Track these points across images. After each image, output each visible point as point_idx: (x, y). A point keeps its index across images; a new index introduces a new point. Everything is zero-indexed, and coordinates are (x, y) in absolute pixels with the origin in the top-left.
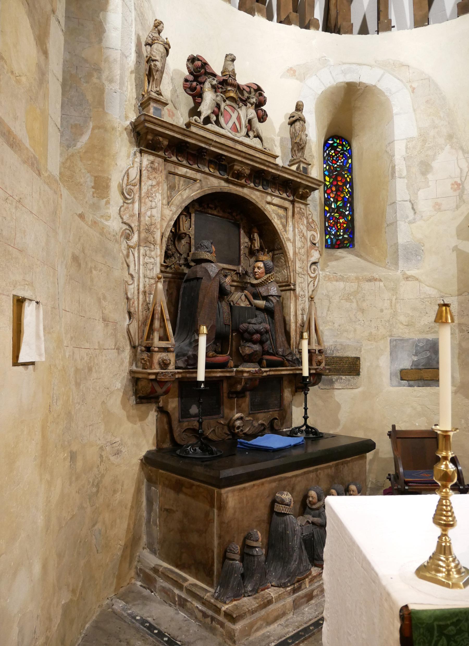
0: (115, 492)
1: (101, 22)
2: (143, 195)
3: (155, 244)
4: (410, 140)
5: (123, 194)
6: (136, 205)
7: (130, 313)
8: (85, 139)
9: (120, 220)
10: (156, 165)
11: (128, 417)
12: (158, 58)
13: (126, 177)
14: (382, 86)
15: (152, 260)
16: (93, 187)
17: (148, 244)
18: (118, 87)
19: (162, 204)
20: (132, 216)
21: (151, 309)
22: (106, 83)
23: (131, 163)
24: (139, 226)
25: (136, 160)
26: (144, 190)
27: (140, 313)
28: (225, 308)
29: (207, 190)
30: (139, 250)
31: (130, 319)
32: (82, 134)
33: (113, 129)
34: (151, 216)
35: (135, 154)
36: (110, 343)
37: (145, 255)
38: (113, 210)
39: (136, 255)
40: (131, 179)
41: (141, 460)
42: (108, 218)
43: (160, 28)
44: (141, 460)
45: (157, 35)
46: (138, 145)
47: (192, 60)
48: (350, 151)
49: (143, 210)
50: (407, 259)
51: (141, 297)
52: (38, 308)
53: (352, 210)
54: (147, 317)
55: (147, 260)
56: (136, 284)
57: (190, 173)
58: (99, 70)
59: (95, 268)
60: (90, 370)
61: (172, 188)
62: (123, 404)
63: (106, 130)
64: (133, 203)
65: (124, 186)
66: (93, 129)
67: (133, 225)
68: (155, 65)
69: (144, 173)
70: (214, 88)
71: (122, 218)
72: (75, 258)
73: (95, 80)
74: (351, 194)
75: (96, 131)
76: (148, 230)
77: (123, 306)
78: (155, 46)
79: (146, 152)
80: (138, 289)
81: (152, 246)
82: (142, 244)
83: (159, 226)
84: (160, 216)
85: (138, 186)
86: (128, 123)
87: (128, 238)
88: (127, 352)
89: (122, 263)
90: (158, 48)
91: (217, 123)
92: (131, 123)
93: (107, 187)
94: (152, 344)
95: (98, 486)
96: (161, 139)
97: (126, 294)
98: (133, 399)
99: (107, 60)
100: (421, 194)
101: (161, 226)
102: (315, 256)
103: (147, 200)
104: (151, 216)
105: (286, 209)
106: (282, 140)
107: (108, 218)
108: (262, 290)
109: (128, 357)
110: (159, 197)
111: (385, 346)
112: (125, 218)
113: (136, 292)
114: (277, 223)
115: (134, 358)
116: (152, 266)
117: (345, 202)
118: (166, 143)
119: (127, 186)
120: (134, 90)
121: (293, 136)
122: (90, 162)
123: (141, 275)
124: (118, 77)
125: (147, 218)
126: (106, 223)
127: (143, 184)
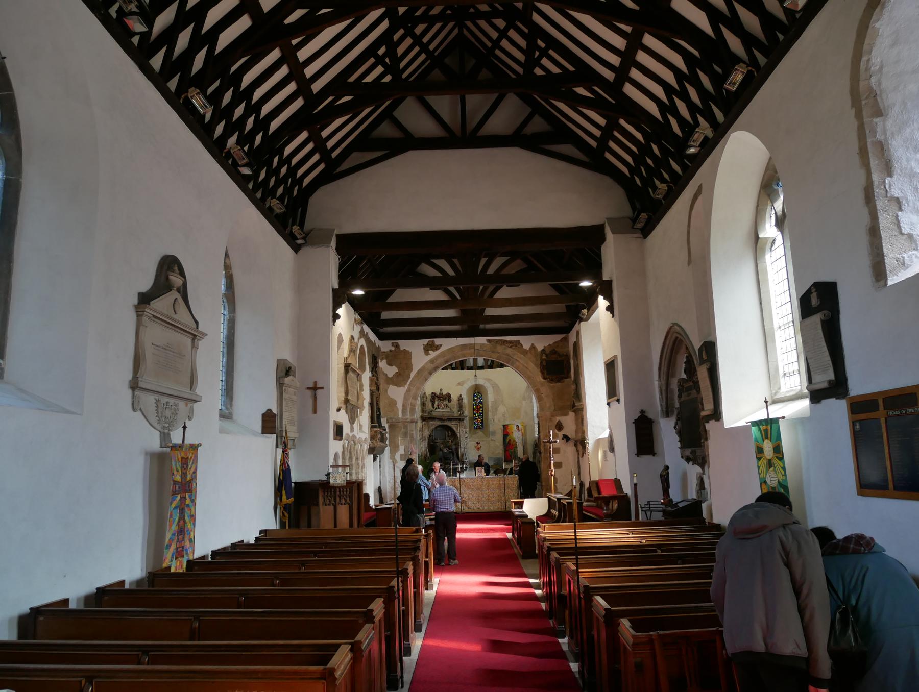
14: (485, 385)
46: (422, 419)
47: (433, 393)
48: (482, 397)
50: (492, 435)
53: (482, 416)
61: (429, 427)
74: (482, 411)
76: (424, 437)
91: (439, 408)
100: (495, 417)
102: (466, 435)
105: (457, 425)
106: (457, 404)
108: (451, 447)
114: (455, 429)
117: (480, 414)
121: (459, 404)
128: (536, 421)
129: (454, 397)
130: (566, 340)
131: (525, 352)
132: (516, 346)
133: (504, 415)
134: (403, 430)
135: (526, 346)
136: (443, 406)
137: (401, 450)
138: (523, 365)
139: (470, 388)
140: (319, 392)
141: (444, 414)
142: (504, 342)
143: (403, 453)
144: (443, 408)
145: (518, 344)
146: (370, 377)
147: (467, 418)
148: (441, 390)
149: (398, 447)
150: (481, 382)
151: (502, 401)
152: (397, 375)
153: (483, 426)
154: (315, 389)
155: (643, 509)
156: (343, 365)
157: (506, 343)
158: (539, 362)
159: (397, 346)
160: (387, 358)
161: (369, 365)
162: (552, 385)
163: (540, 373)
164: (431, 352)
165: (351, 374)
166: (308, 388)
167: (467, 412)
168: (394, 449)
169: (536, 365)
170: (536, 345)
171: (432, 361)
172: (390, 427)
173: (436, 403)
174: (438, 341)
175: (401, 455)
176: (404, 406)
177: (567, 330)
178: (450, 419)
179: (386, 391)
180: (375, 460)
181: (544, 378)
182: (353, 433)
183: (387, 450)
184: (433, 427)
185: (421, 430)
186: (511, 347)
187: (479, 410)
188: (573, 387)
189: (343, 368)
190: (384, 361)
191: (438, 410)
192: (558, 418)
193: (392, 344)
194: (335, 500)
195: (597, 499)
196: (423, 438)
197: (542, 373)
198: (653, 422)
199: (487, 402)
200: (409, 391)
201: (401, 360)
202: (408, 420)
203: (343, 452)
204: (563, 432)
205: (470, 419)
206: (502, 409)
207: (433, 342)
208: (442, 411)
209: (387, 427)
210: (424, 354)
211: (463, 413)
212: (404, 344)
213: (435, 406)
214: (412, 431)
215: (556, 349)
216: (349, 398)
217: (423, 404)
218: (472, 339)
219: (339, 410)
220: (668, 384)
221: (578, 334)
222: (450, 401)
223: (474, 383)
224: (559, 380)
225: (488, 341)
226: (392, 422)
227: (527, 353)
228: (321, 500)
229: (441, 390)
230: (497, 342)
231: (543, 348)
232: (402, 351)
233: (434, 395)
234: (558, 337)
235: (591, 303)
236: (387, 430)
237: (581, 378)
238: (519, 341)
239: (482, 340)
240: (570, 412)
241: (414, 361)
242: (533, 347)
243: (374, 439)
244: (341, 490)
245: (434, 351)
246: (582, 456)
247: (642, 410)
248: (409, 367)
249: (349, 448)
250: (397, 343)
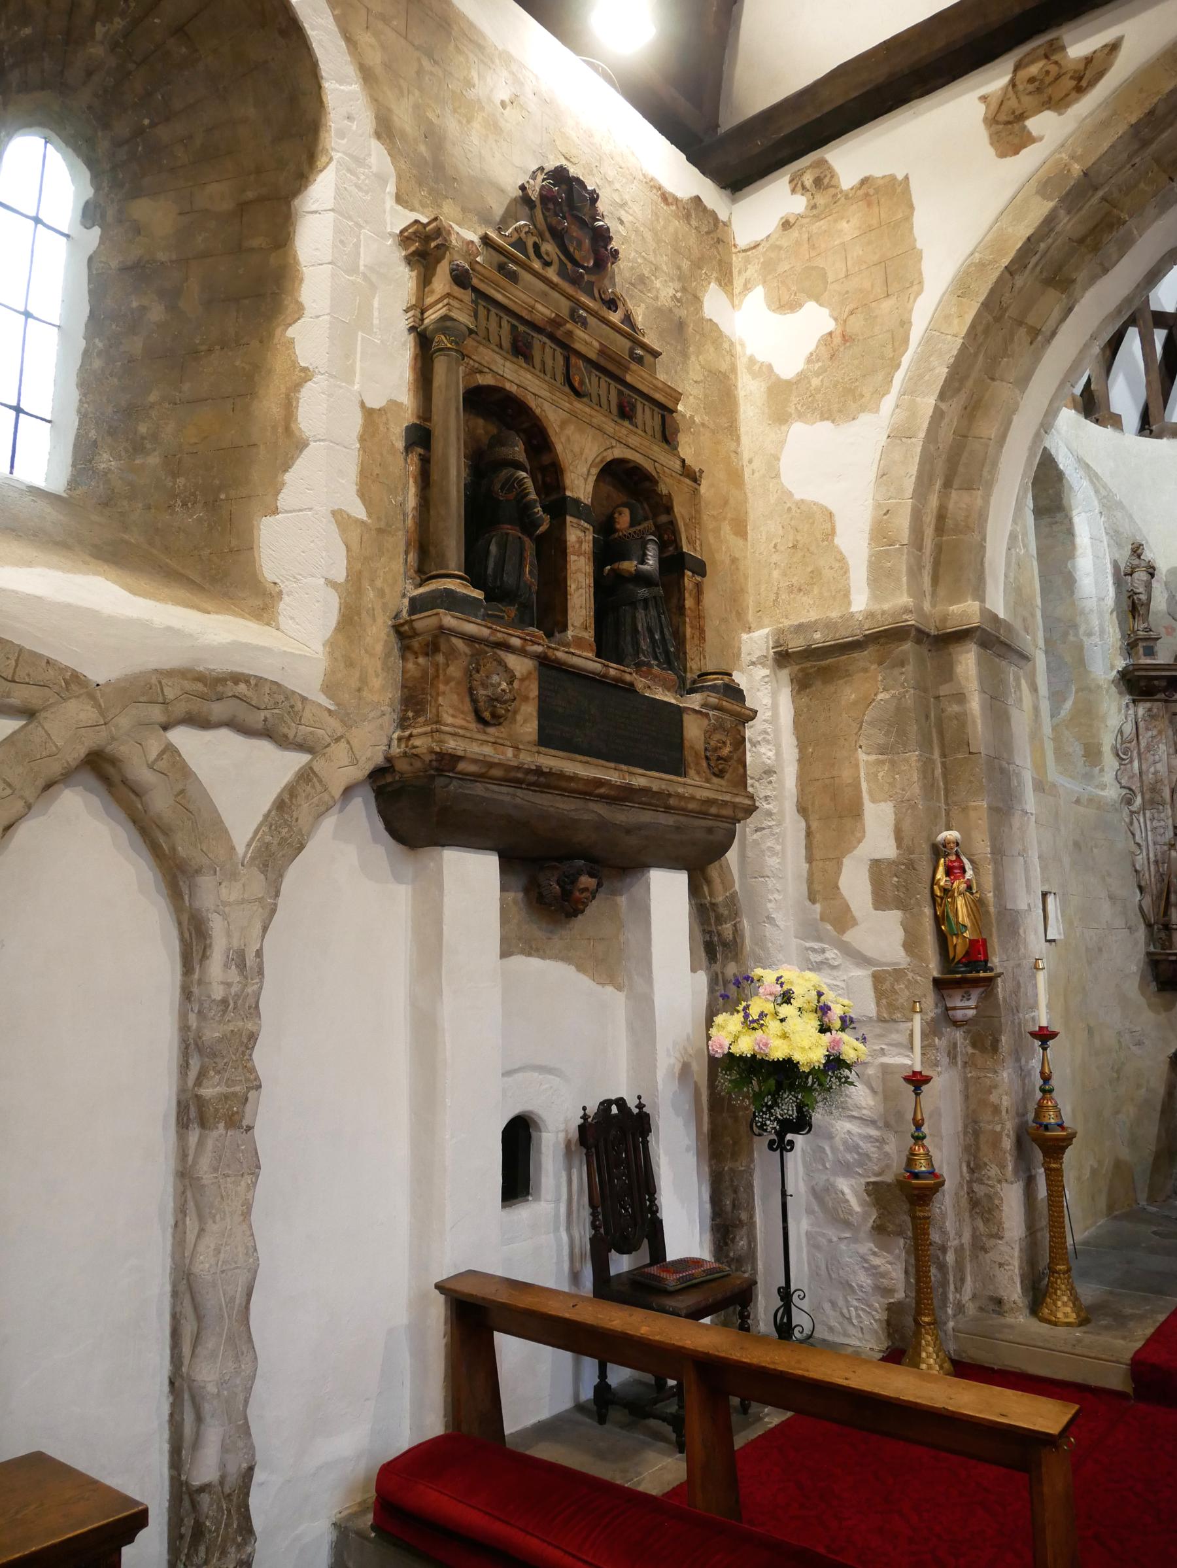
0: (1139, 1086)
1: (1070, 572)
2: (1142, 750)
3: (1163, 804)
5: (1118, 755)
6: (1136, 764)
7: (1141, 888)
8: (1068, 704)
9: (1118, 786)
10: (1155, 710)
11: (1149, 1005)
12: (1141, 590)
13: (1119, 736)
15: (1162, 823)
16: (1084, 756)
17: (1156, 806)
18: (1098, 640)
19: (1168, 755)
20: (1131, 777)
21: (1166, 881)
22: (1085, 639)
23: (1123, 717)
24: (1142, 786)
25: (1130, 712)
26: (1143, 744)
27: (1154, 887)
30: (1144, 814)
31: (1141, 893)
32: (1064, 700)
33: (1099, 687)
34: (1156, 773)
35: (1127, 705)
36: (1119, 922)
37: (1152, 820)
38: (1109, 777)
39: (1142, 820)
40: (1125, 736)
41: (1170, 1058)
42: (1103, 787)
43: (1139, 551)
44: (1170, 1058)
45: (1136, 562)
46: (1131, 693)
49: (1144, 767)
51: (1152, 867)
52: (1055, 898)
54: (1161, 893)
55: (1155, 823)
56: (1145, 854)
58: (1075, 626)
59: (1096, 847)
60: (1100, 950)
62: (1143, 987)
63: (1090, 690)
64: (1131, 762)
65: (1118, 746)
66: (1077, 692)
67: (1134, 788)
68: (1139, 599)
69: (1141, 725)
71: (1120, 783)
72: (1077, 845)
73: (1071, 638)
75: (1080, 694)
76: (1154, 789)
77: (1132, 881)
78: (1136, 575)
79: (1140, 701)
80: (1148, 859)
81: (1161, 807)
82: (1148, 807)
83: (1166, 782)
84: (1166, 770)
85: (1135, 742)
86: (1115, 672)
87: (1129, 802)
88: (1141, 933)
89: (1126, 832)
90: (1141, 575)
92: (1118, 672)
93: (1099, 753)
94: (1170, 920)
95: (1118, 1072)
96: (1156, 683)
97: (1134, 866)
98: (1153, 986)
99: (1082, 613)
101: (1170, 782)
103: (1148, 755)
104: (1156, 773)
107: (1103, 787)
109: (1143, 937)
110: (1163, 747)
112: (1124, 782)
113: (1146, 862)
115: (1151, 938)
116: (1162, 831)
118: (1164, 683)
119: (1122, 744)
120: (1117, 630)
122: (1077, 729)
123: (1150, 843)
124: (1097, 628)
125: (1151, 776)
126: (1102, 793)
127: (1141, 737)
143: (888, 850)
149: (855, 811)
175: (877, 867)
210: (991, 151)
245: (1058, 104)
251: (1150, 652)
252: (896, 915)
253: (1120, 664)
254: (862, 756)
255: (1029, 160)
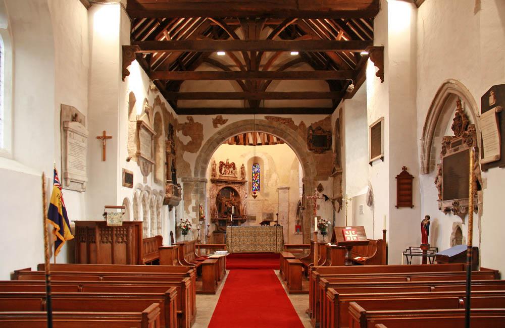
4: (267, 170)
28: (226, 208)
29: (223, 187)
57: (220, 185)
70: (225, 168)
76: (213, 196)
90: (215, 165)
102: (246, 196)
111: (261, 214)
114: (237, 190)
121: (242, 171)
128: (301, 185)
129: (238, 167)
130: (329, 119)
131: (295, 128)
132: (289, 123)
133: (276, 181)
134: (194, 187)
135: (297, 123)
136: (228, 172)
137: (193, 203)
138: (294, 139)
139: (250, 160)
140: (108, 142)
141: (229, 178)
142: (278, 119)
143: (195, 205)
144: (229, 174)
145: (290, 121)
146: (166, 141)
147: (247, 183)
148: (228, 160)
149: (191, 200)
150: (258, 155)
151: (275, 171)
152: (190, 143)
153: (259, 189)
154: (104, 138)
155: (405, 253)
156: (136, 123)
157: (280, 119)
158: (306, 137)
159: (191, 120)
160: (183, 129)
161: (165, 131)
162: (316, 155)
163: (307, 146)
164: (219, 125)
165: (142, 131)
166: (98, 138)
167: (248, 178)
168: (188, 201)
169: (304, 139)
170: (304, 122)
171: (219, 133)
172: (184, 184)
173: (223, 169)
174: (224, 117)
175: (193, 207)
176: (196, 168)
177: (330, 111)
178: (234, 182)
179: (182, 156)
180: (170, 210)
181: (310, 150)
182: (146, 184)
183: (182, 203)
184: (221, 188)
185: (211, 190)
186: (284, 123)
187: (256, 177)
188: (335, 155)
189: (136, 125)
190: (181, 132)
191: (225, 175)
192: (320, 182)
193: (188, 117)
194: (112, 239)
195: (340, 244)
196: (212, 196)
197: (309, 146)
198: (414, 178)
199: (263, 173)
200: (200, 156)
201: (194, 130)
202: (199, 180)
203: (135, 199)
204: (324, 193)
205: (250, 183)
206: (274, 176)
207: (221, 117)
208: (228, 176)
209: (182, 184)
211: (244, 179)
212: (197, 118)
213: (223, 172)
214: (202, 188)
215: (321, 127)
216: (141, 152)
217: (214, 170)
218: (253, 115)
219: (128, 160)
220: (431, 142)
221: (341, 111)
222: (234, 168)
223: (253, 156)
224: (322, 152)
225: (265, 117)
226: (187, 181)
227: (297, 128)
228: (98, 238)
229: (228, 160)
230: (273, 118)
231: (310, 125)
232: (195, 124)
233: (222, 164)
234: (323, 117)
235: (359, 76)
236: (182, 187)
237: (342, 148)
238: (291, 118)
239: (261, 117)
240: (329, 178)
241: (204, 132)
242: (302, 124)
243: (168, 192)
244: (119, 229)
245: (221, 124)
246: (338, 212)
247: (404, 167)
248: (201, 137)
249: (142, 196)
250: (191, 117)
251: (215, 176)
252: (195, 213)
253: (211, 177)
254: (192, 194)
255: (217, 130)
